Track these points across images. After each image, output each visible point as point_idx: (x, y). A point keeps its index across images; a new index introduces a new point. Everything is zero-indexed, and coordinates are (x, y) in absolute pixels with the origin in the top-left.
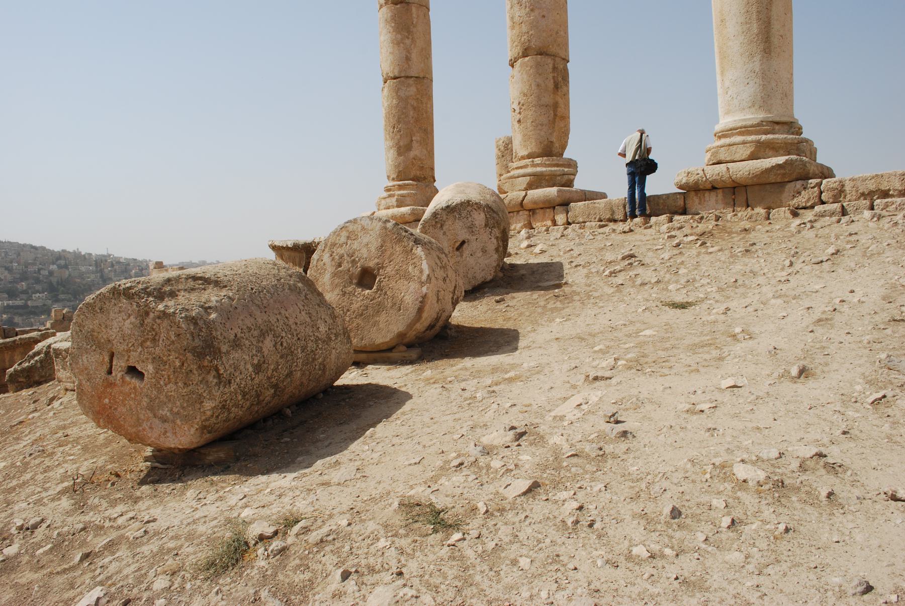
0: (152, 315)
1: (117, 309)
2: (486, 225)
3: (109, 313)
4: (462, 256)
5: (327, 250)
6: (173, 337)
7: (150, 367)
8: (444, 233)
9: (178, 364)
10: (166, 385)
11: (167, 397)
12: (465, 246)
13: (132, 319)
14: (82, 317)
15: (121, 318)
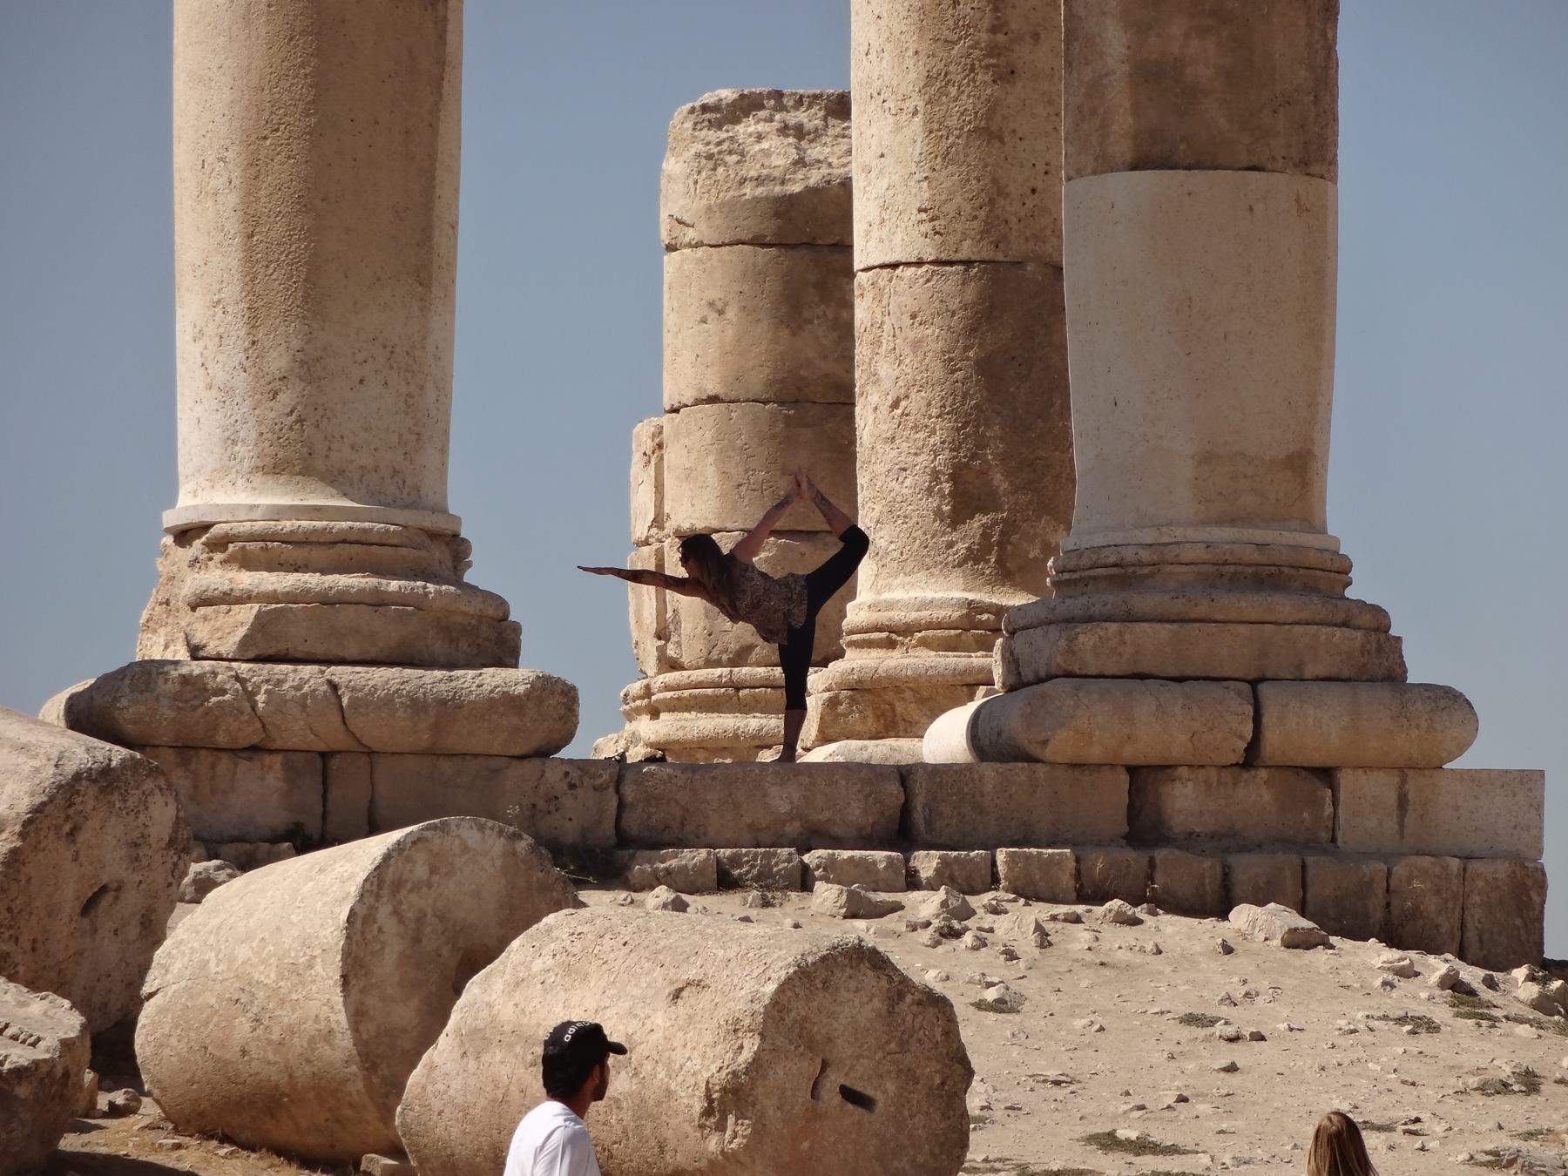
0: (909, 998)
1: (853, 984)
2: (172, 842)
3: (837, 989)
4: (95, 931)
5: (385, 892)
6: (938, 1037)
7: (890, 1086)
8: (75, 860)
9: (938, 1081)
10: (912, 1116)
11: (910, 1137)
12: (107, 899)
13: (877, 1003)
14: (789, 994)
15: (857, 1003)
